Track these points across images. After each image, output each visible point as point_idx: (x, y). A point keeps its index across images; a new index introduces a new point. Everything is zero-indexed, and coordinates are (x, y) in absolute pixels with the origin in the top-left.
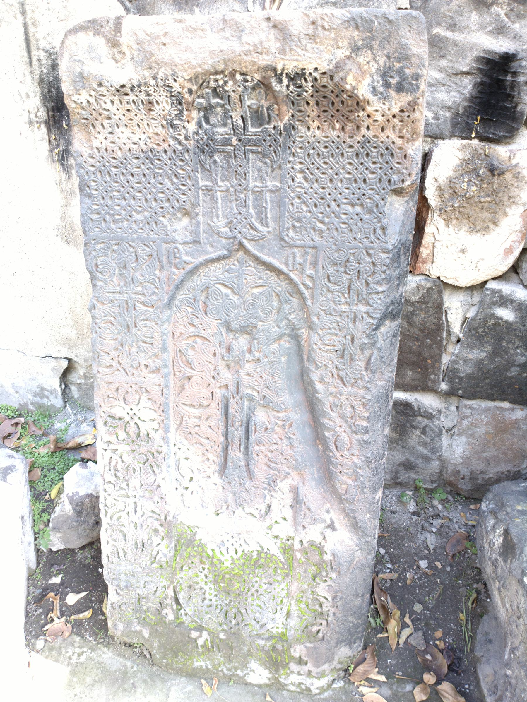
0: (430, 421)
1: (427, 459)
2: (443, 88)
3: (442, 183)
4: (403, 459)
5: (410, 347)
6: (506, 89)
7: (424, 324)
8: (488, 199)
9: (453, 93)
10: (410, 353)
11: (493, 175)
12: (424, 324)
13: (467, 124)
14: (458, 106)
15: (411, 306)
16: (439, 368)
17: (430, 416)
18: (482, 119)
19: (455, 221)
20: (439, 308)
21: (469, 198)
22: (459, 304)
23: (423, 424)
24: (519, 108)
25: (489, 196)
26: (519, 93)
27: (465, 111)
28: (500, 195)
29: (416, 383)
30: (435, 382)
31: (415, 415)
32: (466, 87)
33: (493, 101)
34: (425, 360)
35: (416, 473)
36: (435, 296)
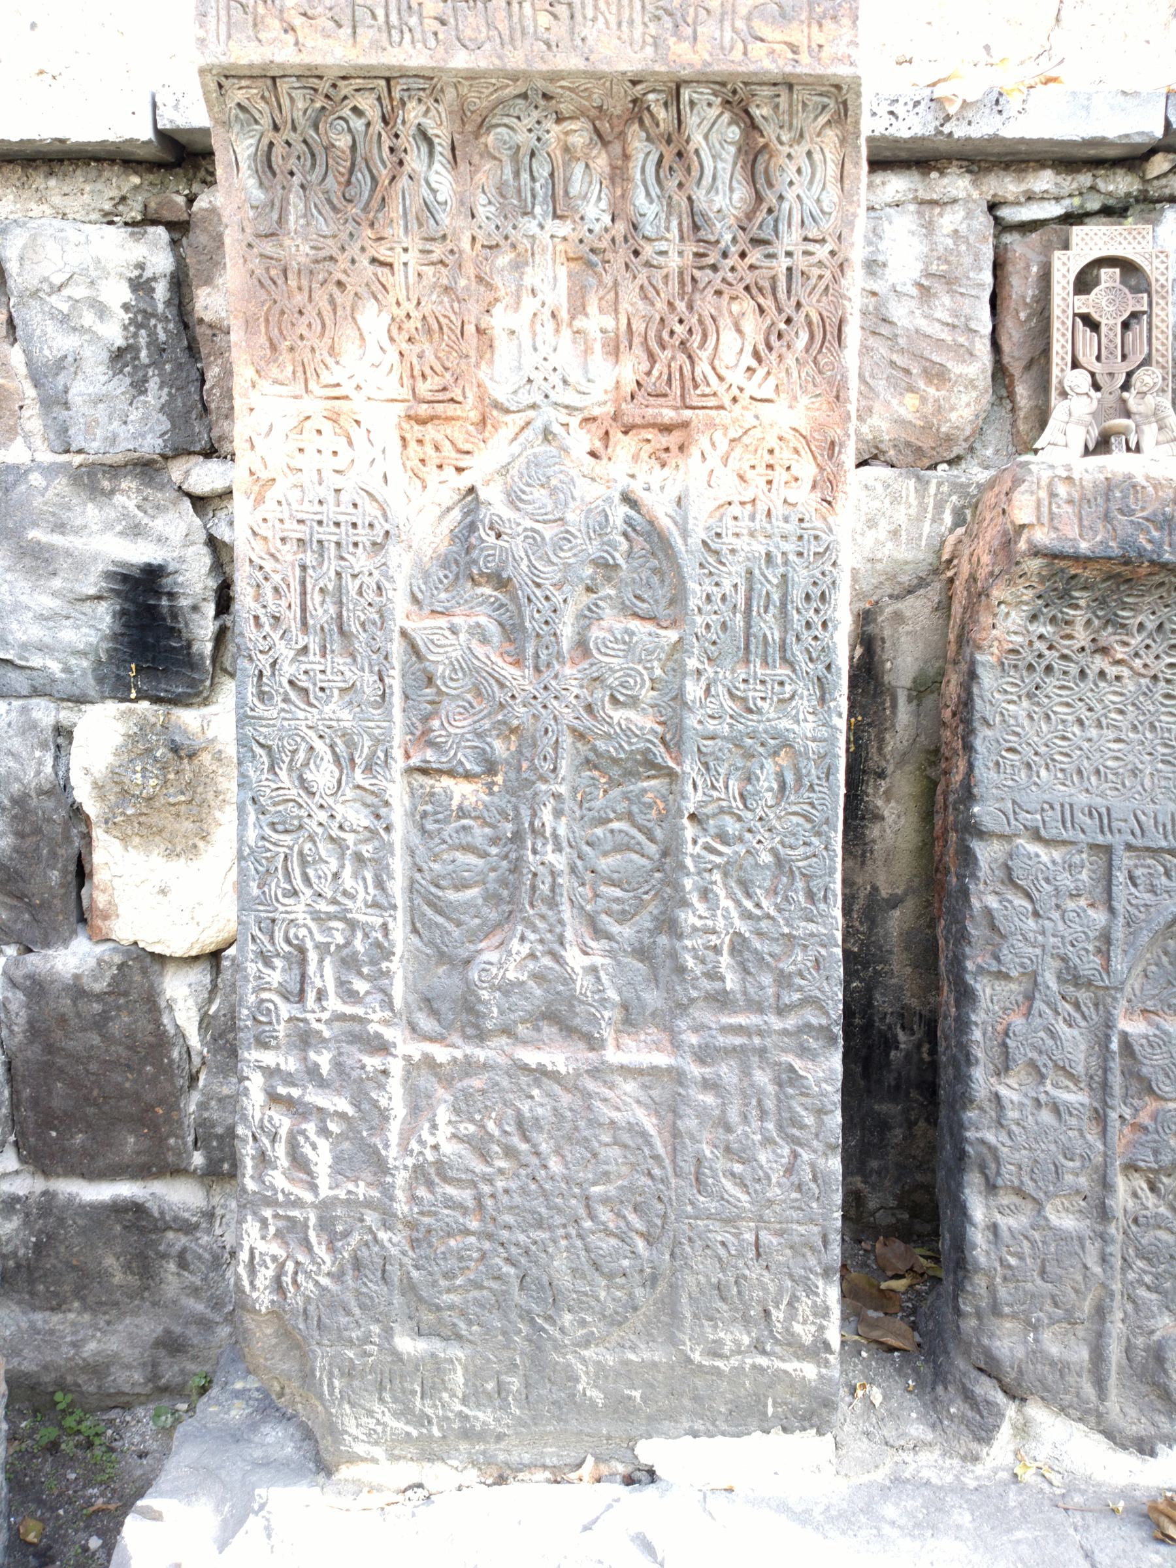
0: (190, 1237)
1: (206, 1325)
2: (68, 623)
3: (97, 775)
4: (160, 1329)
5: (118, 1084)
6: (164, 619)
7: (132, 1035)
8: (183, 798)
9: (84, 630)
10: (122, 1098)
11: (181, 758)
12: (132, 1035)
13: (118, 677)
14: (96, 650)
15: (98, 1001)
16: (180, 1123)
17: (188, 1228)
18: (139, 670)
19: (137, 840)
20: (152, 1003)
21: (150, 799)
22: (187, 991)
23: (178, 1247)
24: (195, 648)
25: (182, 793)
26: (187, 625)
27: (110, 657)
28: (200, 789)
29: (143, 1159)
30: (180, 1154)
31: (156, 1230)
32: (102, 619)
33: (151, 640)
34: (150, 1108)
35: (194, 1358)
36: (138, 978)
